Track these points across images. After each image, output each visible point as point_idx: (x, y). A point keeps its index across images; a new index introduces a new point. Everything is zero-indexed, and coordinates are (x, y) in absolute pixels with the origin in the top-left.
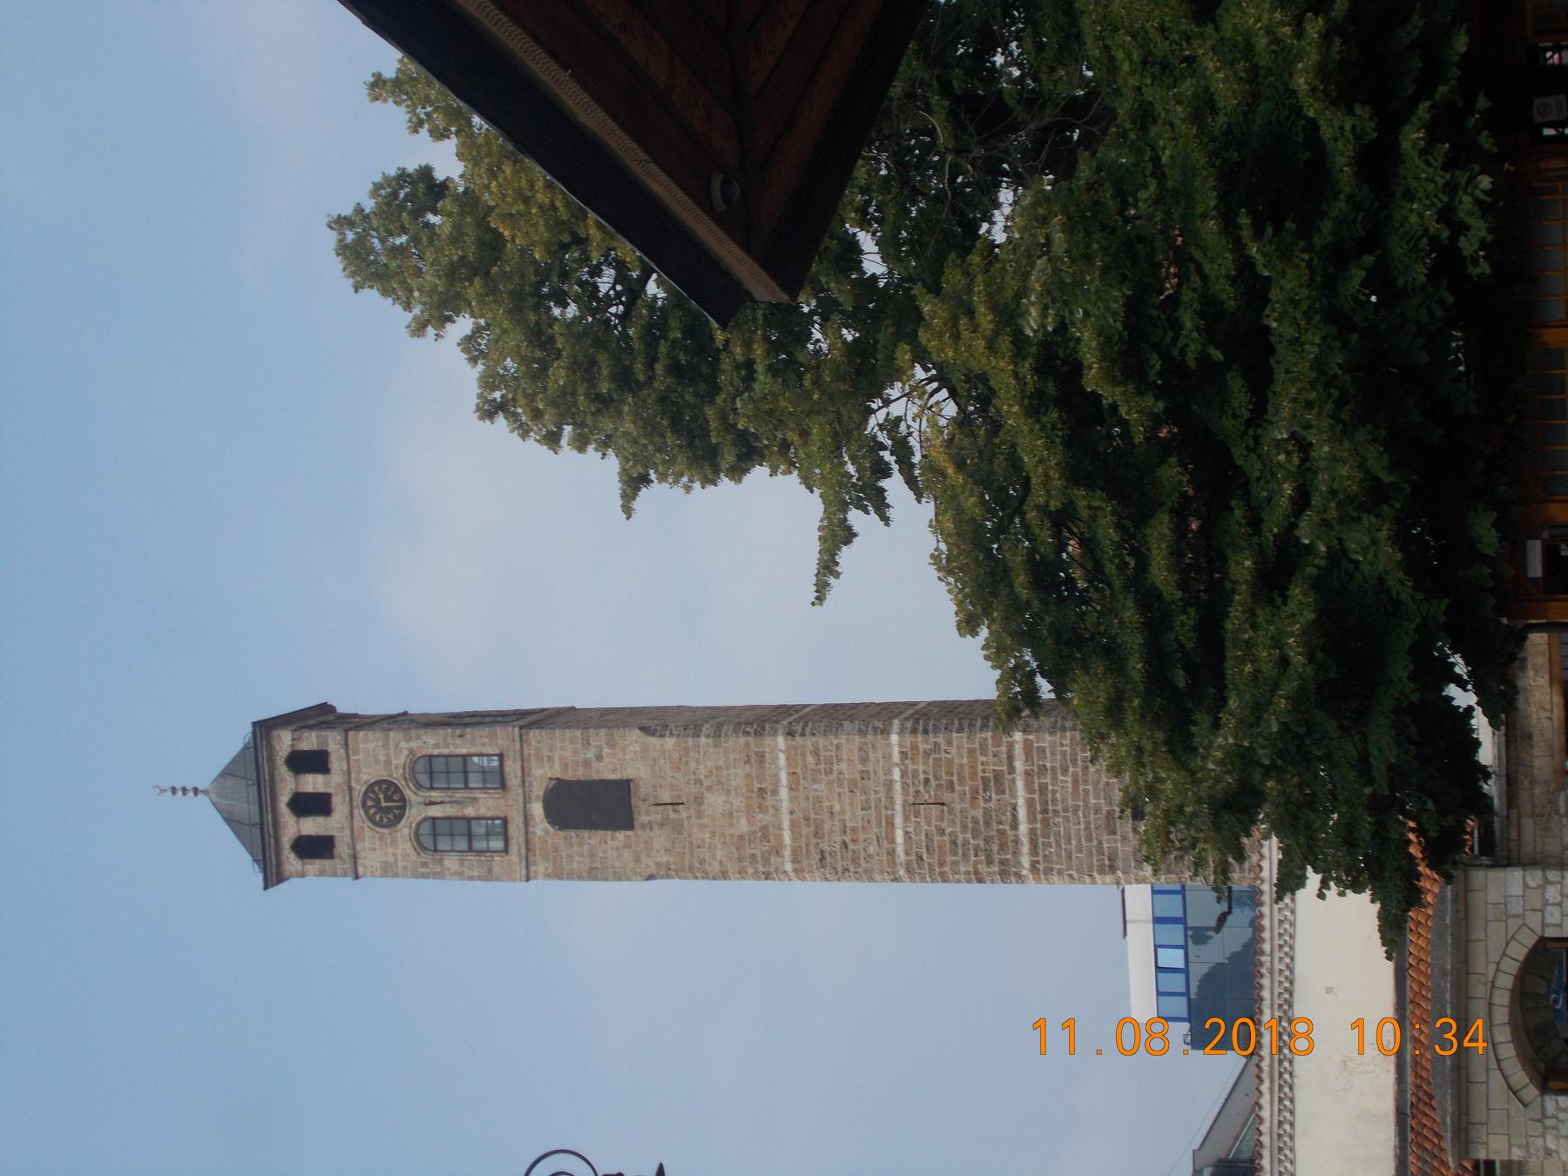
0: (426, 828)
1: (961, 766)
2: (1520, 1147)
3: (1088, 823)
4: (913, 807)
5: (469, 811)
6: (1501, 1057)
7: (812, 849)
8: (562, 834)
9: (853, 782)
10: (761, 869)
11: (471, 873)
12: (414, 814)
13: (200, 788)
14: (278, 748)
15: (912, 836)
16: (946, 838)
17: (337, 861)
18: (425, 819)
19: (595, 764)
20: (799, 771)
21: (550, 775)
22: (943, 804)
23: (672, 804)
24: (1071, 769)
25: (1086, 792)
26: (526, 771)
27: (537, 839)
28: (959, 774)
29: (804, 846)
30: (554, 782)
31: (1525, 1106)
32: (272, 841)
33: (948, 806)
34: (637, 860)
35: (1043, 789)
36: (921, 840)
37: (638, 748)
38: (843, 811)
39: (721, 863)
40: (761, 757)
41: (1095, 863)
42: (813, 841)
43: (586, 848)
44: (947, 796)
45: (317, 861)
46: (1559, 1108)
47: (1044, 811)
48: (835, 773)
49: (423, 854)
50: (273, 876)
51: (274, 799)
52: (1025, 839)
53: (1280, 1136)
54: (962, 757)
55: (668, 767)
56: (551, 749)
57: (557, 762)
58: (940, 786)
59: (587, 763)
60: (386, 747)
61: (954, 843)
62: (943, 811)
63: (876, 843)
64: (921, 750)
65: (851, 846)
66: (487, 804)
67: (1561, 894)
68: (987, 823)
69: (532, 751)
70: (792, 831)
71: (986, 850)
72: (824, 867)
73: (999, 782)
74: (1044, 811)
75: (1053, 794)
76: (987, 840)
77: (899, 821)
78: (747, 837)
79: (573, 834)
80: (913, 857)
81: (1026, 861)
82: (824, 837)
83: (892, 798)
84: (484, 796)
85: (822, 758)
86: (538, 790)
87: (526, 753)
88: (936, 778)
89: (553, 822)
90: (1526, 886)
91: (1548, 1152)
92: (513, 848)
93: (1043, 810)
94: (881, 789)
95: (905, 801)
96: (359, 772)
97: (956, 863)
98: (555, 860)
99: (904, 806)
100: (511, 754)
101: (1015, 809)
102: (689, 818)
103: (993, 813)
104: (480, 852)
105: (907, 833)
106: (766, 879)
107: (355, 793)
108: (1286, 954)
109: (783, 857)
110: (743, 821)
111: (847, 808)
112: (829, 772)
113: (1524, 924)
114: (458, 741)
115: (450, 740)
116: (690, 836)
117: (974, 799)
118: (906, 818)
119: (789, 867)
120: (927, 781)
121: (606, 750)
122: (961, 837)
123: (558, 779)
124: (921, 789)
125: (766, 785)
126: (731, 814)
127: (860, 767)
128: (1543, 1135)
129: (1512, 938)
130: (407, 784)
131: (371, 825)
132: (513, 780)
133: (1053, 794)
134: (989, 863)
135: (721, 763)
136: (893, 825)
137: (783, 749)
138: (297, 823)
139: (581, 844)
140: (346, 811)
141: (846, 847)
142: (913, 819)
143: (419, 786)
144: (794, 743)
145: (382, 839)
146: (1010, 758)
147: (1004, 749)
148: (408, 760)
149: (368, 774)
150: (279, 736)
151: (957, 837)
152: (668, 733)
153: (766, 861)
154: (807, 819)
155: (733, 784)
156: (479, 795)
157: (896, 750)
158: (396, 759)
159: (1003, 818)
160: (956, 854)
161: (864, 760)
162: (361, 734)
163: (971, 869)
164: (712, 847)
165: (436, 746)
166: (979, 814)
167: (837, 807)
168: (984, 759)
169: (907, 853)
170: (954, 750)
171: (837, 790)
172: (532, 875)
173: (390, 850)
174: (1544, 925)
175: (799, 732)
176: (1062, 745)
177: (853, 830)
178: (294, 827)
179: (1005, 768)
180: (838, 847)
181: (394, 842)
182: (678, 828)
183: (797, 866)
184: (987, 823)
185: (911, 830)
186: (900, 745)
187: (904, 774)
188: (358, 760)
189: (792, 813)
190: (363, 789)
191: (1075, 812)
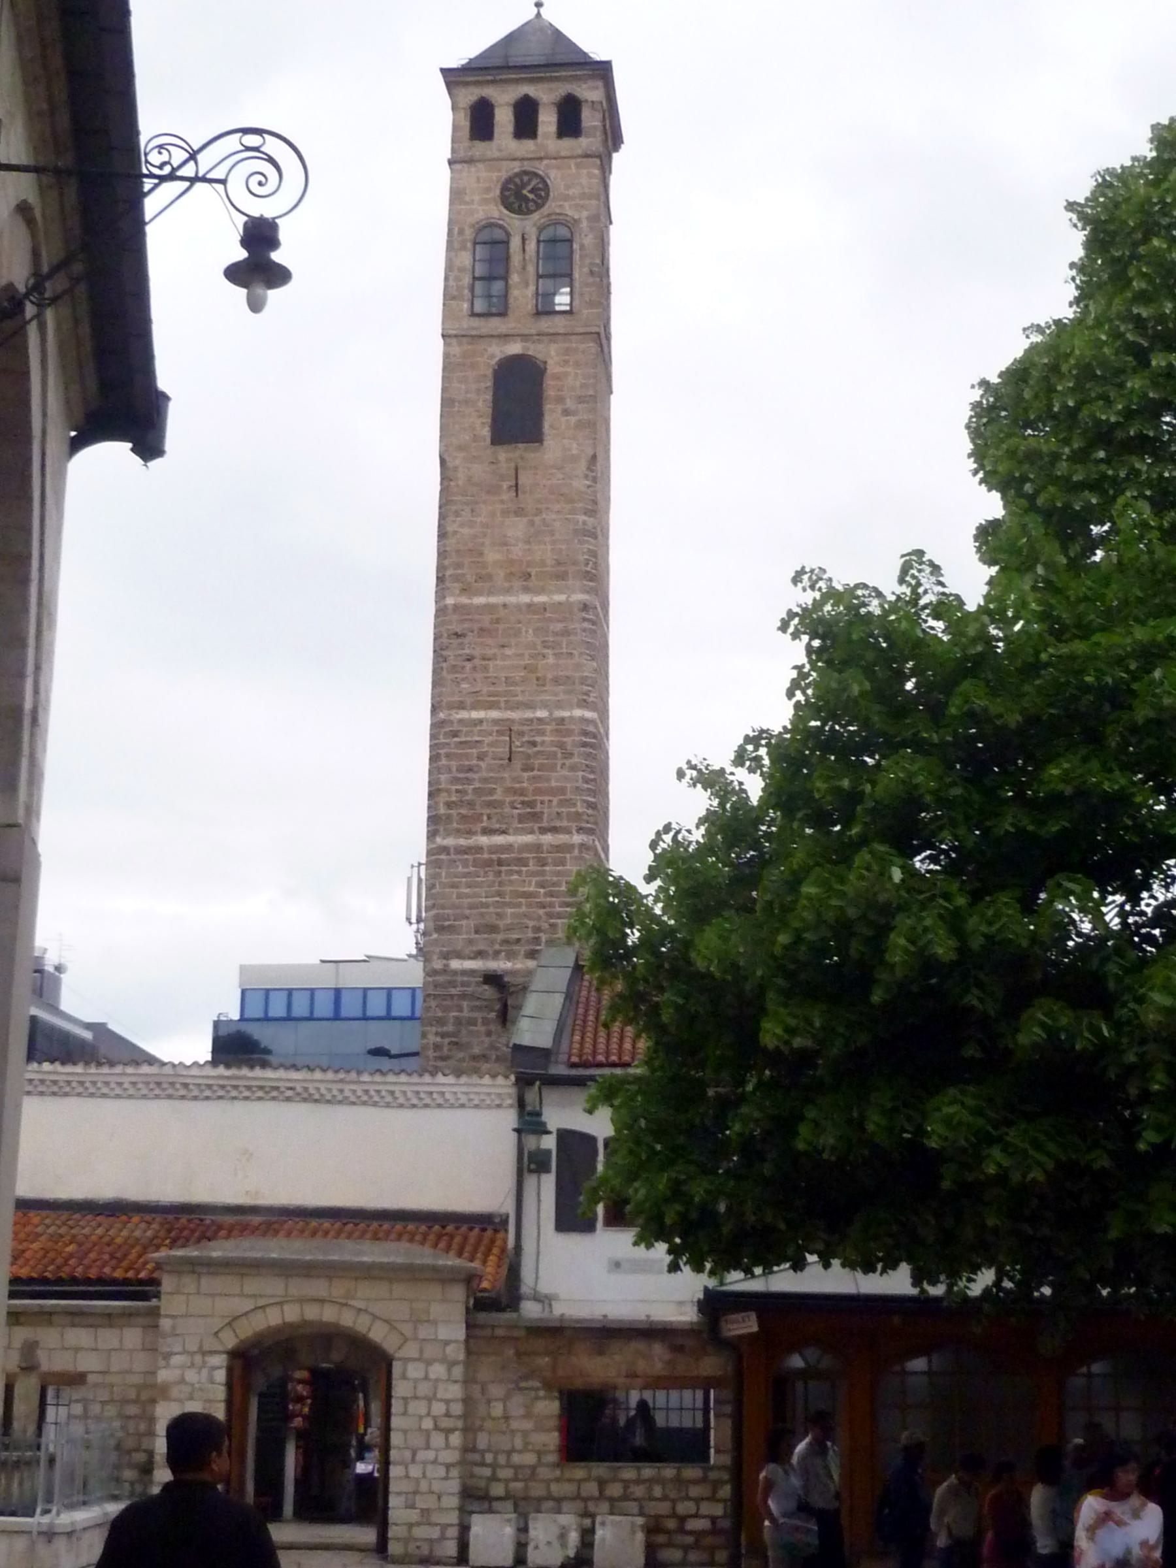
0: (498, 234)
1: (548, 780)
2: (174, 1327)
3: (486, 906)
4: (507, 729)
5: (515, 278)
6: (268, 1310)
7: (466, 625)
8: (490, 372)
11: (451, 278)
12: (515, 223)
13: (542, 10)
14: (584, 86)
15: (478, 728)
16: (475, 762)
17: (467, 143)
18: (508, 234)
19: (559, 408)
20: (548, 615)
21: (550, 362)
22: (510, 759)
24: (542, 891)
25: (519, 905)
28: (540, 777)
29: (470, 617)
30: (542, 366)
31: (216, 1334)
32: (490, 78)
33: (508, 765)
34: (461, 448)
35: (523, 862)
37: (575, 452)
39: (455, 532)
40: (562, 576)
41: (446, 911)
42: (476, 626)
43: (472, 396)
44: (517, 764)
45: (468, 124)
46: (214, 1368)
47: (500, 863)
50: (453, 78)
51: (532, 81)
53: (172, 1084)
56: (577, 364)
57: (562, 369)
58: (528, 757)
59: (560, 400)
60: (583, 196)
62: (501, 759)
64: (565, 740)
65: (468, 665)
66: (522, 295)
67: (437, 1380)
68: (490, 804)
69: (574, 345)
71: (461, 801)
72: (449, 637)
73: (531, 817)
74: (500, 863)
75: (517, 872)
76: (471, 804)
77: (494, 714)
78: (480, 560)
79: (489, 384)
80: (456, 727)
81: (450, 842)
82: (479, 637)
85: (559, 638)
86: (535, 350)
87: (573, 338)
90: (446, 1343)
91: (167, 1356)
92: (476, 322)
93: (498, 861)
95: (513, 721)
96: (558, 168)
97: (450, 771)
98: (464, 365)
99: (508, 720)
101: (504, 832)
102: (502, 502)
103: (498, 811)
104: (472, 289)
105: (481, 721)
106: (437, 578)
107: (536, 163)
109: (458, 596)
110: (498, 556)
112: (545, 645)
113: (406, 1340)
114: (586, 270)
115: (587, 261)
116: (485, 502)
117: (515, 792)
118: (496, 722)
119: (450, 601)
120: (534, 744)
121: (573, 420)
122: (476, 776)
124: (526, 739)
125: (533, 583)
126: (505, 544)
127: (549, 676)
128: (185, 1352)
132: (545, 324)
133: (517, 872)
134: (449, 805)
135: (557, 536)
136: (490, 708)
137: (571, 600)
138: (508, 104)
139: (478, 391)
140: (519, 154)
141: (469, 660)
143: (541, 229)
144: (576, 610)
145: (488, 190)
146: (554, 830)
147: (565, 823)
148: (568, 219)
149: (556, 178)
150: (597, 88)
152: (588, 483)
153: (457, 578)
154: (498, 621)
156: (532, 288)
157: (566, 714)
159: (494, 820)
161: (556, 681)
162: (597, 172)
164: (471, 524)
165: (582, 247)
166: (498, 796)
167: (508, 652)
168: (555, 803)
169: (461, 721)
171: (527, 653)
172: (448, 340)
173: (477, 198)
174: (407, 1360)
175: (587, 616)
177: (486, 668)
178: (503, 101)
179: (545, 824)
181: (485, 201)
182: (493, 490)
183: (450, 610)
184: (490, 804)
185: (484, 727)
186: (571, 718)
188: (570, 167)
189: (505, 605)
190: (541, 173)
191: (500, 894)
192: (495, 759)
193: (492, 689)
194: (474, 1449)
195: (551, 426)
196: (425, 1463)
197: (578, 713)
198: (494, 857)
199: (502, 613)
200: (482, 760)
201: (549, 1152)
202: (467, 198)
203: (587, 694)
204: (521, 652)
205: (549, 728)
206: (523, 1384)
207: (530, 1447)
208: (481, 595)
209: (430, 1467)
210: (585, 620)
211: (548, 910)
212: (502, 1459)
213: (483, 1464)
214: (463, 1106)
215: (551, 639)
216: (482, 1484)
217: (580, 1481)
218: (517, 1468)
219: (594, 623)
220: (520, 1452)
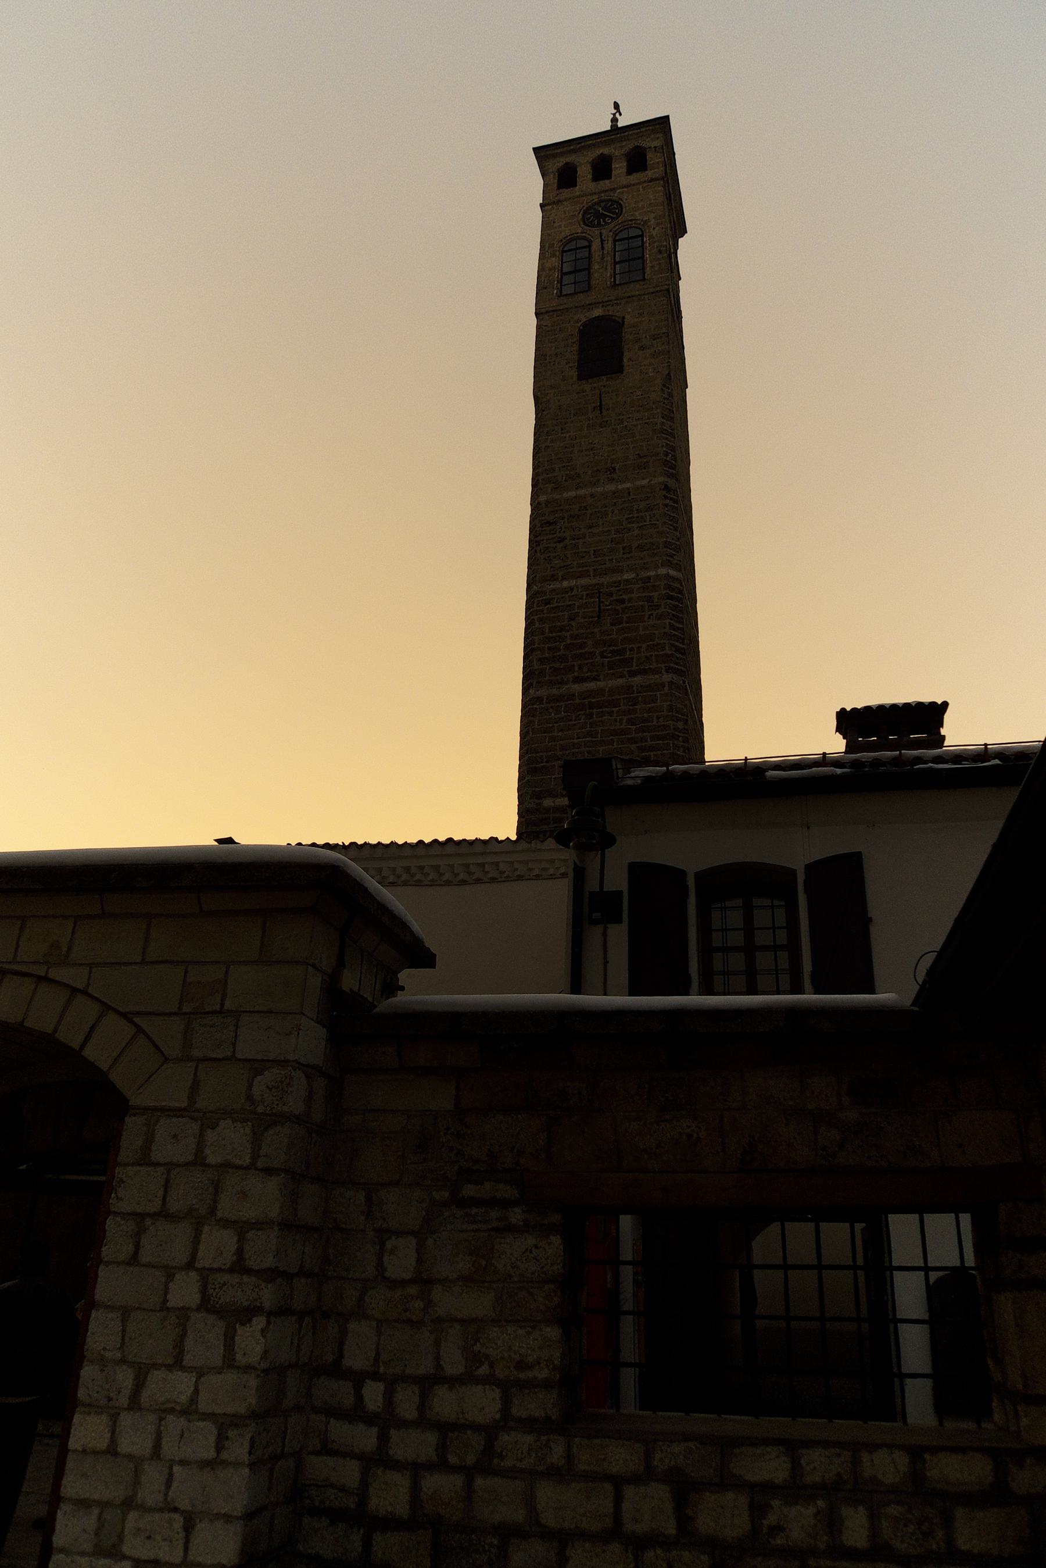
22: (599, 617)
23: (601, 405)
30: (621, 321)
47: (591, 706)
52: (563, 690)
61: (562, 629)
62: (592, 617)
63: (562, 565)
65: (559, 546)
67: (227, 1165)
81: (543, 692)
83: (606, 574)
84: (609, 274)
87: (646, 297)
89: (584, 325)
95: (602, 585)
102: (589, 419)
105: (572, 589)
108: (399, 877)
120: (622, 601)
122: (568, 634)
124: (615, 597)
129: (139, 1030)
130: (619, 224)
134: (541, 661)
141: (559, 542)
146: (644, 672)
154: (586, 508)
157: (652, 573)
159: (585, 670)
160: (551, 632)
165: (651, 237)
176: (658, 718)
179: (634, 668)
187: (628, 582)
192: (585, 618)
194: (335, 1370)
195: (630, 360)
196: (164, 1411)
197: (662, 571)
198: (586, 701)
200: (573, 619)
201: (620, 893)
203: (671, 556)
206: (469, 1191)
207: (484, 1370)
209: (174, 1424)
210: (666, 497)
211: (639, 745)
212: (407, 1404)
213: (357, 1414)
214: (520, 878)
216: (349, 1473)
217: (618, 1482)
218: (446, 1429)
219: (676, 502)
220: (454, 1382)
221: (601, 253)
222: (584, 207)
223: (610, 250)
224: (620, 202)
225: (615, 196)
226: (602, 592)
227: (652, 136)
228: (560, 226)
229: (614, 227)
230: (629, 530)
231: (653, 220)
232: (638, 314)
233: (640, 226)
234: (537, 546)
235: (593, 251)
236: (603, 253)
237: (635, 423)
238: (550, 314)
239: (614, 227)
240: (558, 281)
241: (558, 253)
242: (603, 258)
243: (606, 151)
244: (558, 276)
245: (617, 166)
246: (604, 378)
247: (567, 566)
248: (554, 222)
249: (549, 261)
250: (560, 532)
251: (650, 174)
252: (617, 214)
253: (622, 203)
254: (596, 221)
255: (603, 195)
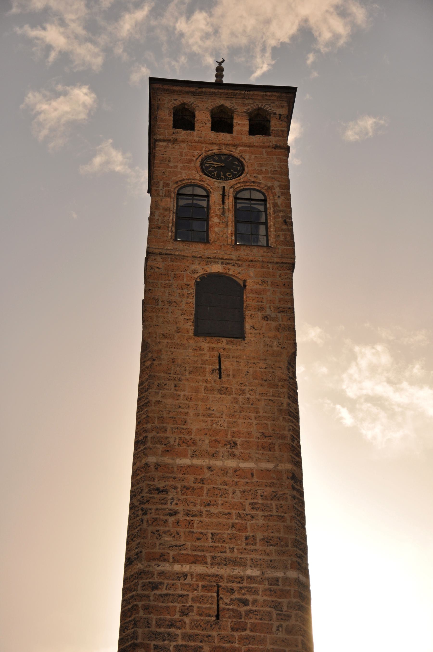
1: (262, 641)
9: (244, 529)
10: (150, 435)
11: (157, 214)
15: (182, 581)
16: (177, 616)
20: (255, 479)
22: (218, 617)
26: (254, 263)
27: (187, 264)
28: (253, 638)
29: (173, 475)
30: (241, 283)
36: (176, 589)
38: (210, 515)
48: (253, 512)
49: (175, 186)
54: (273, 644)
55: (258, 369)
57: (263, 287)
61: (171, 625)
62: (210, 616)
63: (174, 543)
65: (171, 520)
70: (189, 466)
72: (150, 492)
77: (199, 569)
80: (156, 580)
82: (183, 494)
83: (225, 565)
84: (230, 232)
87: (270, 265)
88: (248, 613)
89: (202, 278)
94: (235, 554)
95: (221, 577)
100: (270, 254)
102: (206, 381)
105: (185, 575)
111: (215, 520)
118: (202, 577)
120: (245, 603)
121: (273, 324)
122: (179, 632)
123: (245, 286)
124: (236, 596)
126: (210, 415)
130: (241, 182)
131: (203, 155)
136: (194, 562)
137: (279, 468)
141: (171, 515)
142: (200, 584)
144: (285, 477)
151: (179, 628)
154: (202, 481)
155: (240, 421)
158: (263, 177)
163: (139, 641)
167: (213, 510)
169: (161, 573)
170: (281, 635)
177: (190, 523)
180: (172, 507)
186: (286, 579)
192: (201, 615)
193: (197, 544)
195: (252, 327)
199: (207, 474)
200: (187, 614)
202: (171, 164)
204: (227, 511)
205: (261, 587)
208: (185, 456)
215: (260, 501)
221: (221, 207)
222: (202, 154)
223: (231, 206)
224: (242, 160)
225: (237, 153)
226: (221, 586)
227: (277, 103)
228: (176, 167)
229: (236, 184)
230: (253, 517)
231: (278, 188)
232: (262, 281)
233: (263, 190)
234: (143, 514)
235: (211, 203)
236: (223, 207)
237: (258, 397)
238: (164, 256)
239: (236, 184)
240: (173, 223)
241: (173, 195)
242: (223, 213)
243: (228, 104)
244: (173, 219)
245: (239, 122)
246: (224, 340)
247: (180, 546)
248: (169, 161)
249: (163, 200)
250: (171, 503)
251: (274, 140)
252: (238, 171)
253: (244, 161)
254: (216, 173)
255: (223, 147)
